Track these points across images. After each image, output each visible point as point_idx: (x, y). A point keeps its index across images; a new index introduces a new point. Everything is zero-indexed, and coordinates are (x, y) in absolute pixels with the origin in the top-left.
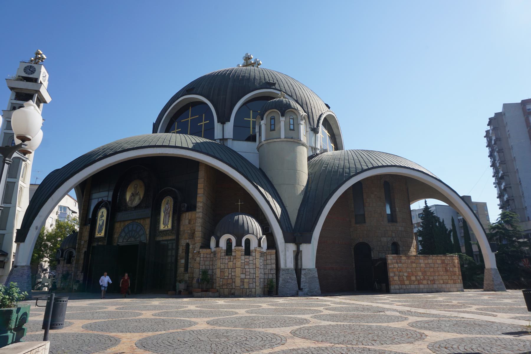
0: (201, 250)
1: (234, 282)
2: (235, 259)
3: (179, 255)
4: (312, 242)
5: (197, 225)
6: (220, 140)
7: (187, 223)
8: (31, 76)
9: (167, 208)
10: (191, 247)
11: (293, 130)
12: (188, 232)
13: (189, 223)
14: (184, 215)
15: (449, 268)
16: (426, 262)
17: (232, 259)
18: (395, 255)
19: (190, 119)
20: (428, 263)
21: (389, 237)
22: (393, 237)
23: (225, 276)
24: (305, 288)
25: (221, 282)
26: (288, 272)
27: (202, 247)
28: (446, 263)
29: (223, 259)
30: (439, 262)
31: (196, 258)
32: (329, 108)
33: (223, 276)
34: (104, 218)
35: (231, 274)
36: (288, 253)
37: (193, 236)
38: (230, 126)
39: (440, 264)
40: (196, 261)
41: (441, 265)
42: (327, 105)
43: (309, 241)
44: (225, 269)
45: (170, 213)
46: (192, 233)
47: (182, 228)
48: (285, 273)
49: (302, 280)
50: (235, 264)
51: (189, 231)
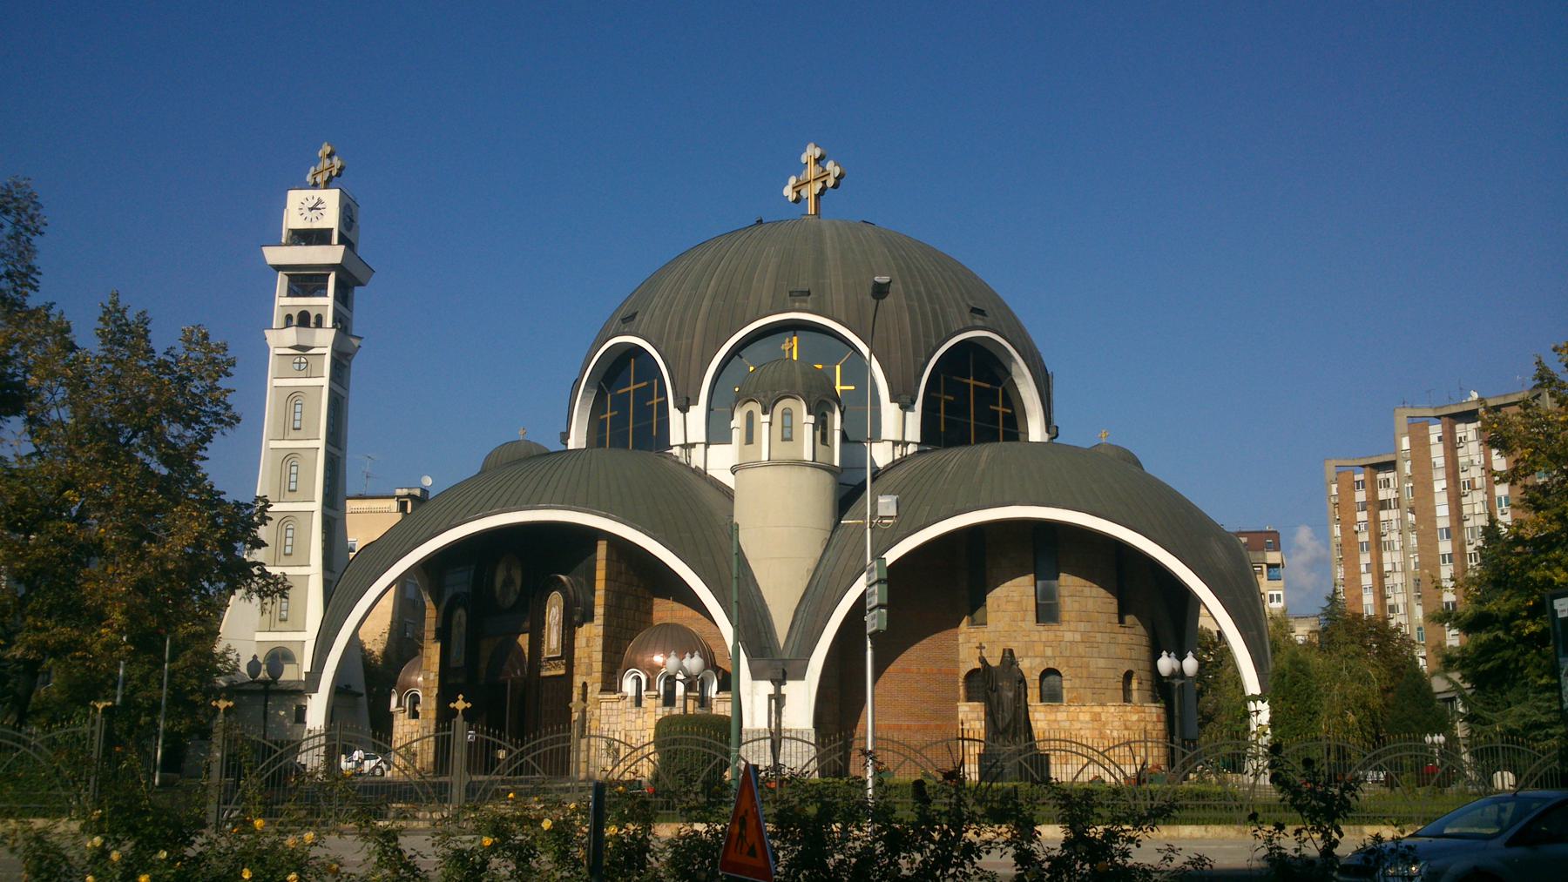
0: (600, 697)
4: (806, 677)
5: (594, 649)
6: (681, 446)
7: (584, 645)
8: (317, 225)
10: (589, 690)
11: (791, 439)
13: (588, 646)
15: (1108, 732)
16: (1052, 717)
18: (976, 703)
19: (632, 388)
20: (1055, 721)
21: (1036, 657)
22: (1045, 657)
27: (603, 690)
28: (1103, 719)
30: (1085, 717)
32: (981, 312)
34: (463, 630)
36: (756, 698)
38: (698, 413)
39: (1087, 722)
41: (1090, 725)
42: (974, 310)
43: (800, 675)
47: (577, 653)
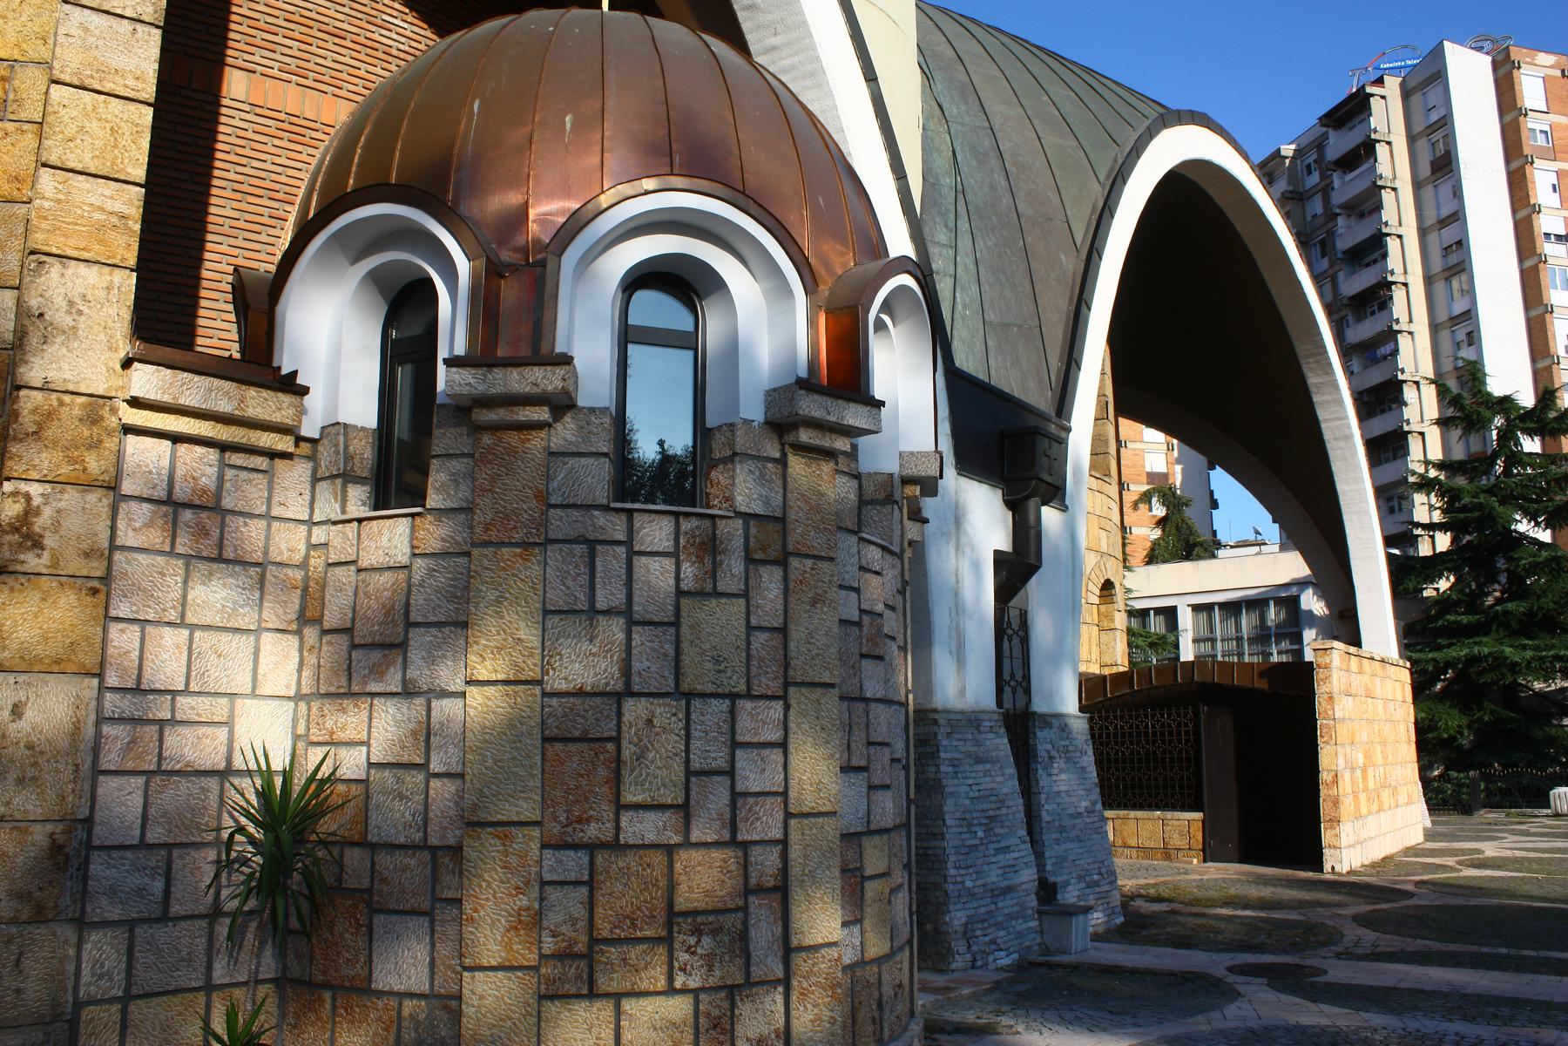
1: (760, 890)
2: (782, 561)
17: (735, 565)
23: (637, 807)
24: (1065, 877)
25: (554, 894)
26: (977, 743)
29: (592, 544)
31: (35, 490)
33: (607, 812)
35: (731, 773)
40: (37, 544)
44: (634, 710)
48: (968, 755)
49: (1046, 817)
50: (783, 631)
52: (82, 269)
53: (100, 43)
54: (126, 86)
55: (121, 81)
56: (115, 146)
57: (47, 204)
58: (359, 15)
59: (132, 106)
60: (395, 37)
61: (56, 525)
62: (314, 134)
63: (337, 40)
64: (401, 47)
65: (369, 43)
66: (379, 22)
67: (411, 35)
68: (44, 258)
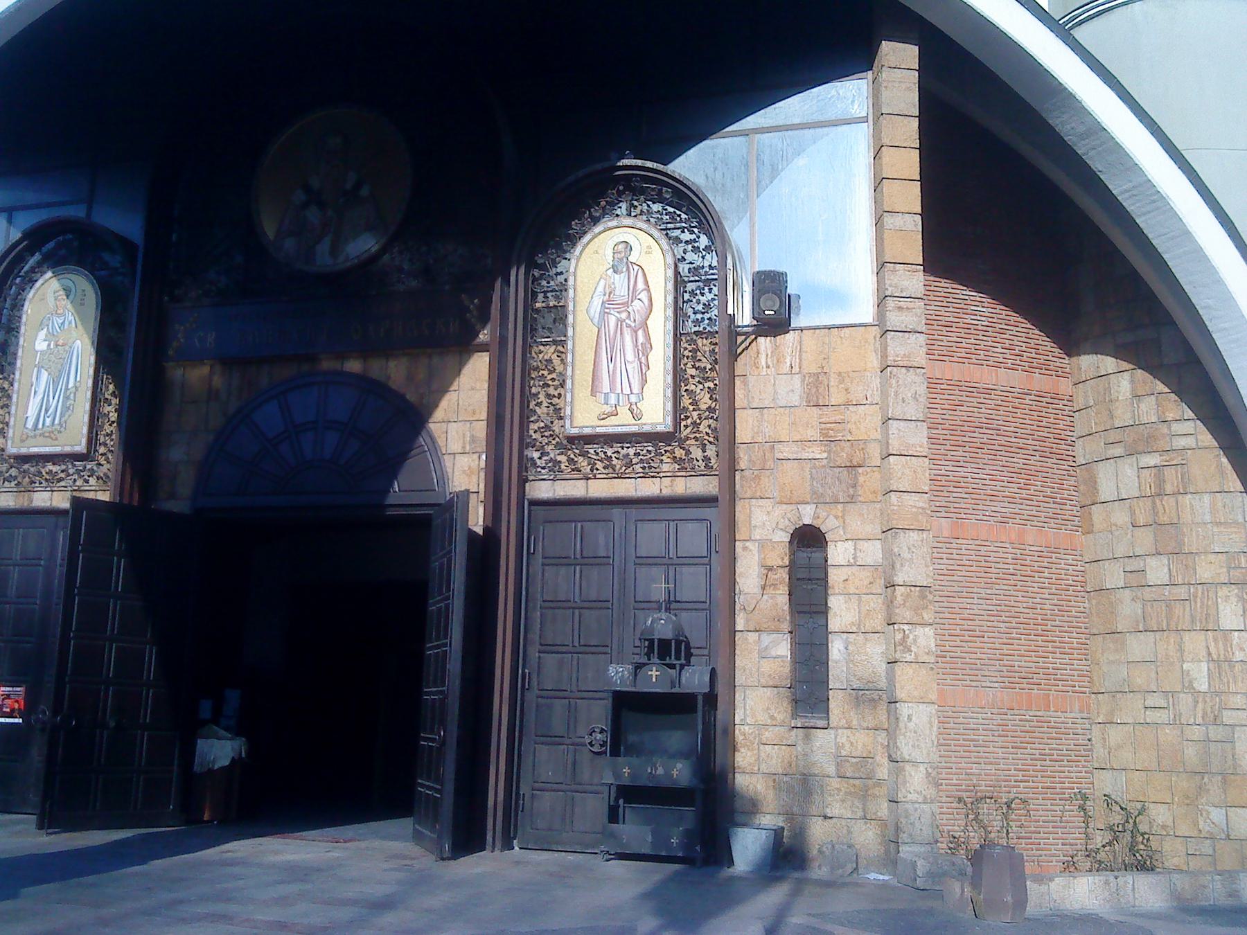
3: (740, 600)
7: (795, 399)
9: (621, 291)
10: (838, 553)
12: (805, 455)
13: (815, 401)
14: (764, 343)
37: (854, 486)
45: (648, 322)
46: (843, 458)
51: (817, 452)
52: (911, 533)
53: (905, 434)
54: (916, 451)
55: (914, 449)
56: (916, 478)
57: (895, 508)
58: (958, 310)
59: (920, 459)
60: (979, 318)
61: (915, 641)
62: (942, 387)
63: (948, 329)
64: (983, 323)
65: (966, 326)
66: (969, 311)
67: (988, 315)
68: (897, 531)
